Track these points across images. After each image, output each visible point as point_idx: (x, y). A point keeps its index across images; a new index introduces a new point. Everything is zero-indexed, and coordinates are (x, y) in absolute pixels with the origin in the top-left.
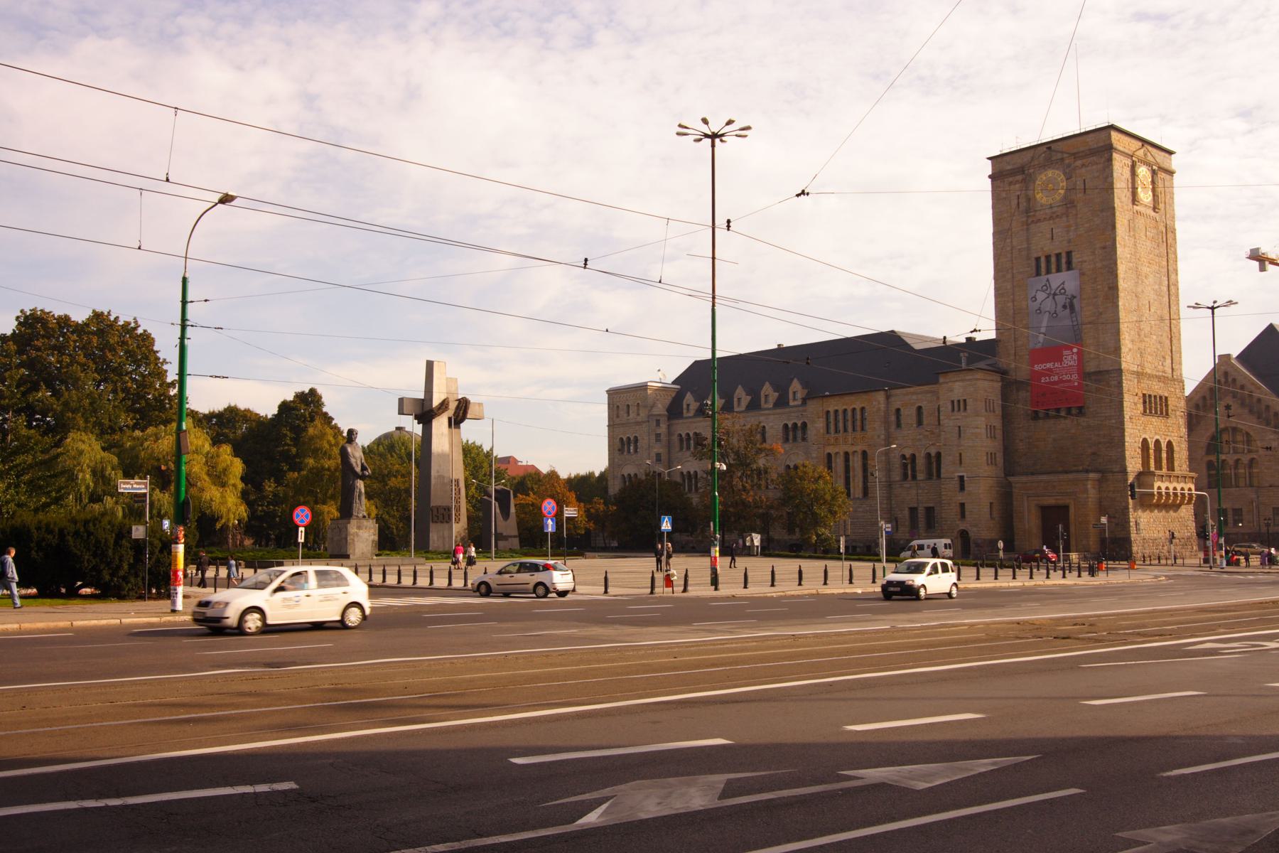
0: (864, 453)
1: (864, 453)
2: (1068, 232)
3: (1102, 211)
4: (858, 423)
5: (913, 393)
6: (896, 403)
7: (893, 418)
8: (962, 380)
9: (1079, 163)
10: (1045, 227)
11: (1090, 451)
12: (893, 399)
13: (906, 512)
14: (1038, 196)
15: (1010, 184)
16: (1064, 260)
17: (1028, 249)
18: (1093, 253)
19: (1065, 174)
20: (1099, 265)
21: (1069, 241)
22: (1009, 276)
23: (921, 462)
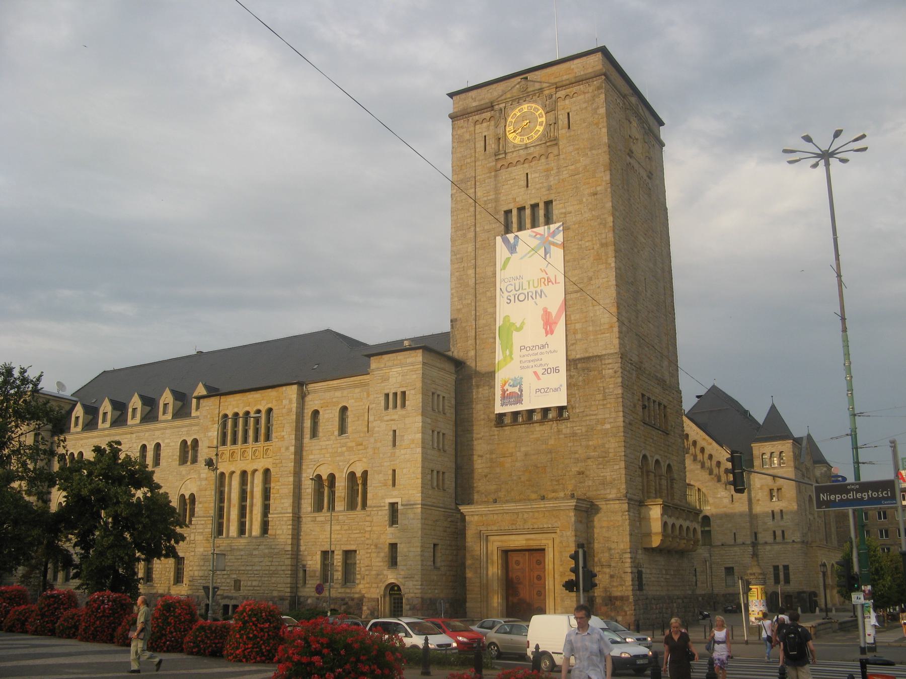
0: (267, 472)
1: (267, 472)
2: (548, 177)
3: (591, 149)
4: (263, 431)
5: (336, 389)
6: (312, 403)
7: (308, 423)
8: (401, 365)
9: (562, 93)
10: (518, 172)
11: (575, 469)
12: (308, 398)
13: (318, 557)
14: (511, 136)
15: (476, 122)
16: (541, 212)
17: (496, 200)
18: (581, 202)
19: (544, 107)
20: (588, 215)
21: (550, 188)
22: (471, 235)
23: (341, 485)
